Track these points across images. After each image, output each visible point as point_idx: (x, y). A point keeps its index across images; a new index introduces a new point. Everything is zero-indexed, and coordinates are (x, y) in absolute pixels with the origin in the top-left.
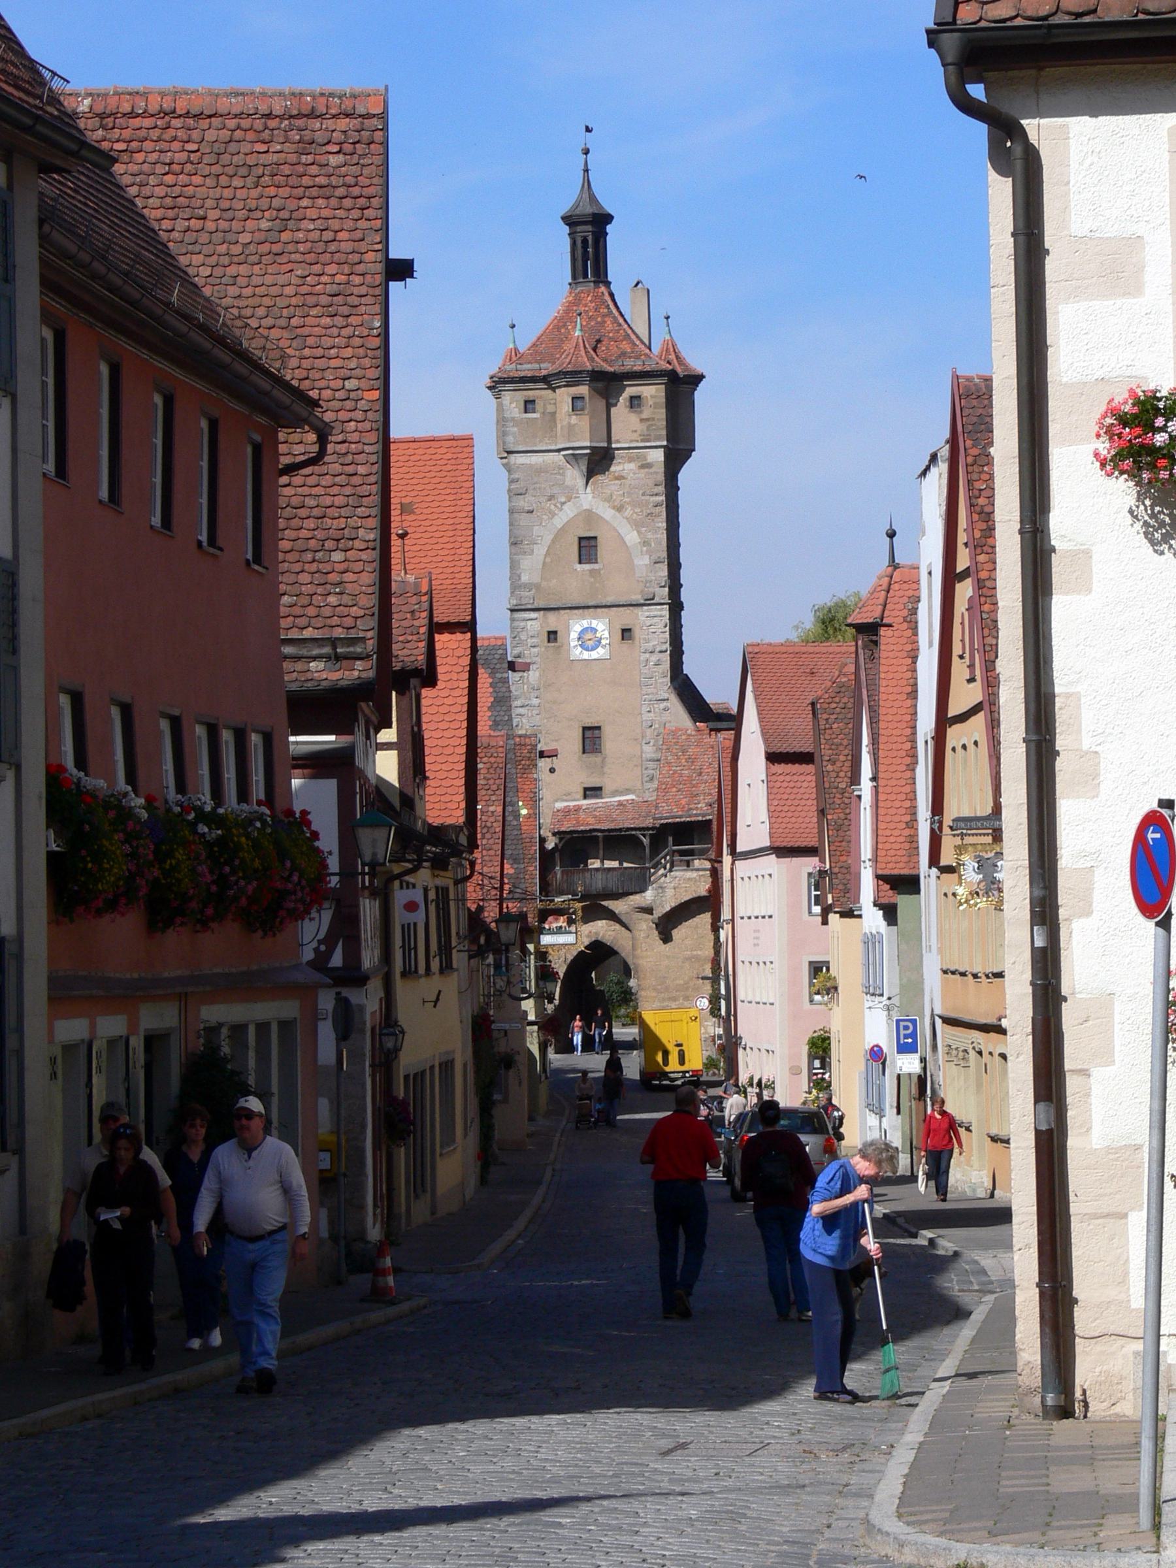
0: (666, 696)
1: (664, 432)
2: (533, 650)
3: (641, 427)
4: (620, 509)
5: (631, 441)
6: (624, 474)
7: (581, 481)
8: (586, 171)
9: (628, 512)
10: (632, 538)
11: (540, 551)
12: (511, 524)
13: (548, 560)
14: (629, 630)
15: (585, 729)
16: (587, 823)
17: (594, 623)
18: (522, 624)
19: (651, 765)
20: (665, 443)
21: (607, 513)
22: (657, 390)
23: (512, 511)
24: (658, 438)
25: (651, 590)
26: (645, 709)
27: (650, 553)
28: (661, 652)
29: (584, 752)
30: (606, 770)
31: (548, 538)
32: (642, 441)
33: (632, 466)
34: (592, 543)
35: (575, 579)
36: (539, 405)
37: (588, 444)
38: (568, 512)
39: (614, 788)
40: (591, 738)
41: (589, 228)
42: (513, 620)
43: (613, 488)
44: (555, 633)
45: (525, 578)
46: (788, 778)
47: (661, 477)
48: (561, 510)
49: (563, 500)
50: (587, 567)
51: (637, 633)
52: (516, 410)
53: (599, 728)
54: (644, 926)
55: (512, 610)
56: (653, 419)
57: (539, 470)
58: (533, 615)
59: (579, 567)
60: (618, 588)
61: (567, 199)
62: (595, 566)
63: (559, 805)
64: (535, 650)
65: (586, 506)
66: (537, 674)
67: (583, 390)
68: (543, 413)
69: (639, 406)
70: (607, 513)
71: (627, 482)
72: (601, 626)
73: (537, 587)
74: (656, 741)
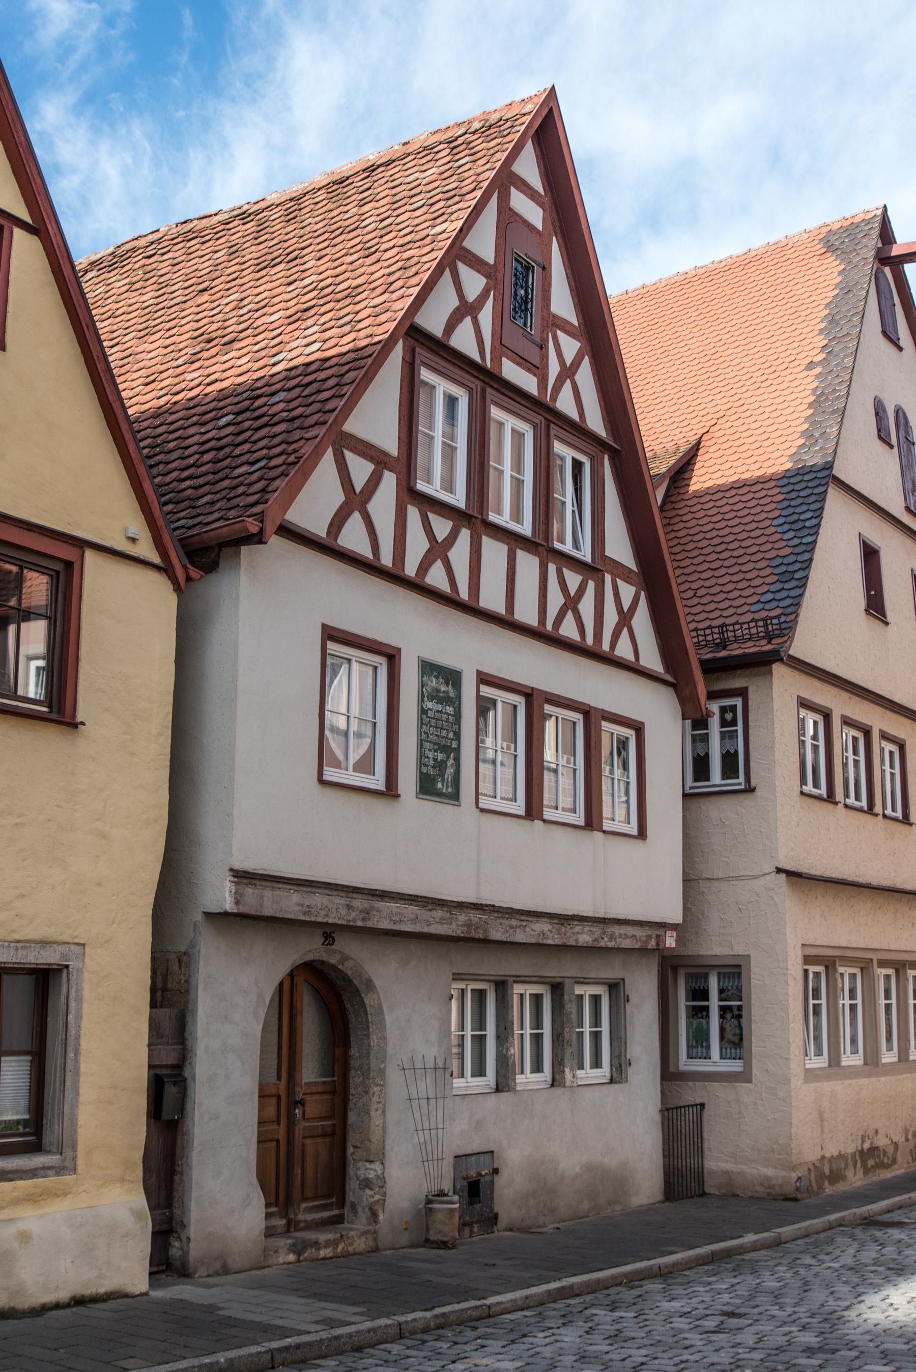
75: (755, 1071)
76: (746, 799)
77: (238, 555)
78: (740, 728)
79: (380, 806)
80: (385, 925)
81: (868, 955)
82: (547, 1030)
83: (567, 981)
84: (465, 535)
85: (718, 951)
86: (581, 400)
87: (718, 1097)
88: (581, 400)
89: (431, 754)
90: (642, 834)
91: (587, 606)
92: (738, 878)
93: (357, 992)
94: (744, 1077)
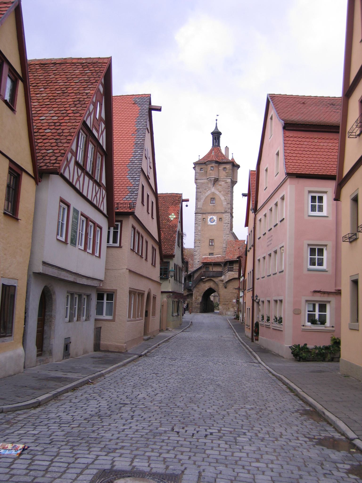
3: (226, 174)
4: (220, 192)
8: (216, 124)
9: (222, 193)
10: (223, 198)
11: (202, 201)
16: (209, 261)
21: (217, 193)
23: (196, 192)
24: (229, 177)
27: (226, 201)
31: (204, 198)
33: (223, 183)
38: (209, 192)
45: (198, 207)
46: (295, 139)
51: (223, 219)
54: (221, 285)
57: (203, 183)
59: (211, 204)
61: (213, 129)
63: (203, 257)
70: (217, 193)
72: (215, 218)
73: (201, 208)
75: (116, 319)
76: (119, 250)
77: (49, 176)
78: (119, 230)
79: (63, 245)
80: (63, 278)
81: (135, 291)
82: (69, 306)
83: (83, 294)
84: (83, 174)
85: (108, 288)
86: (103, 141)
87: (105, 326)
88: (103, 141)
89: (73, 233)
90: (99, 257)
91: (98, 195)
92: (116, 269)
93: (51, 295)
94: (113, 320)
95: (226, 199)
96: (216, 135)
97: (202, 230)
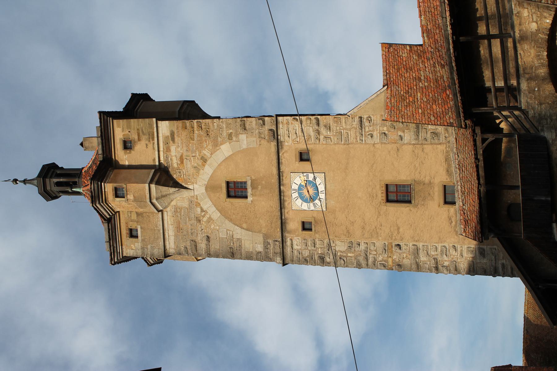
0: (357, 119)
1: (147, 120)
2: (317, 246)
3: (143, 142)
4: (204, 160)
5: (154, 148)
6: (179, 156)
7: (184, 193)
8: (25, 182)
9: (206, 153)
10: (226, 150)
11: (239, 233)
12: (217, 256)
13: (245, 226)
14: (301, 154)
15: (388, 201)
17: (295, 187)
18: (295, 252)
19: (422, 135)
20: (154, 120)
21: (208, 171)
22: (119, 126)
23: (209, 255)
25: (266, 132)
26: (369, 140)
27: (237, 135)
28: (318, 124)
29: (409, 202)
30: (427, 181)
31: (229, 225)
32: (153, 140)
33: (173, 148)
34: (232, 185)
35: (260, 203)
36: (133, 225)
37: (147, 185)
38: (207, 204)
39: (444, 172)
40: (398, 195)
41: (47, 180)
42: (292, 261)
43: (189, 166)
44: (303, 223)
45: (260, 248)
47: (179, 123)
48: (206, 212)
49: (199, 210)
50: (249, 191)
52: (136, 244)
53: (387, 186)
55: (284, 264)
56: (138, 130)
57: (179, 229)
58: (289, 243)
59: (250, 199)
60: (264, 165)
62: (249, 183)
64: (318, 242)
65: (203, 190)
66: (338, 243)
67: (108, 188)
68: (137, 222)
69: (131, 142)
70: (208, 171)
71: (185, 154)
72: (297, 180)
73: (266, 237)
74: (399, 129)
95: (230, 136)
96: (54, 181)
97: (348, 233)
